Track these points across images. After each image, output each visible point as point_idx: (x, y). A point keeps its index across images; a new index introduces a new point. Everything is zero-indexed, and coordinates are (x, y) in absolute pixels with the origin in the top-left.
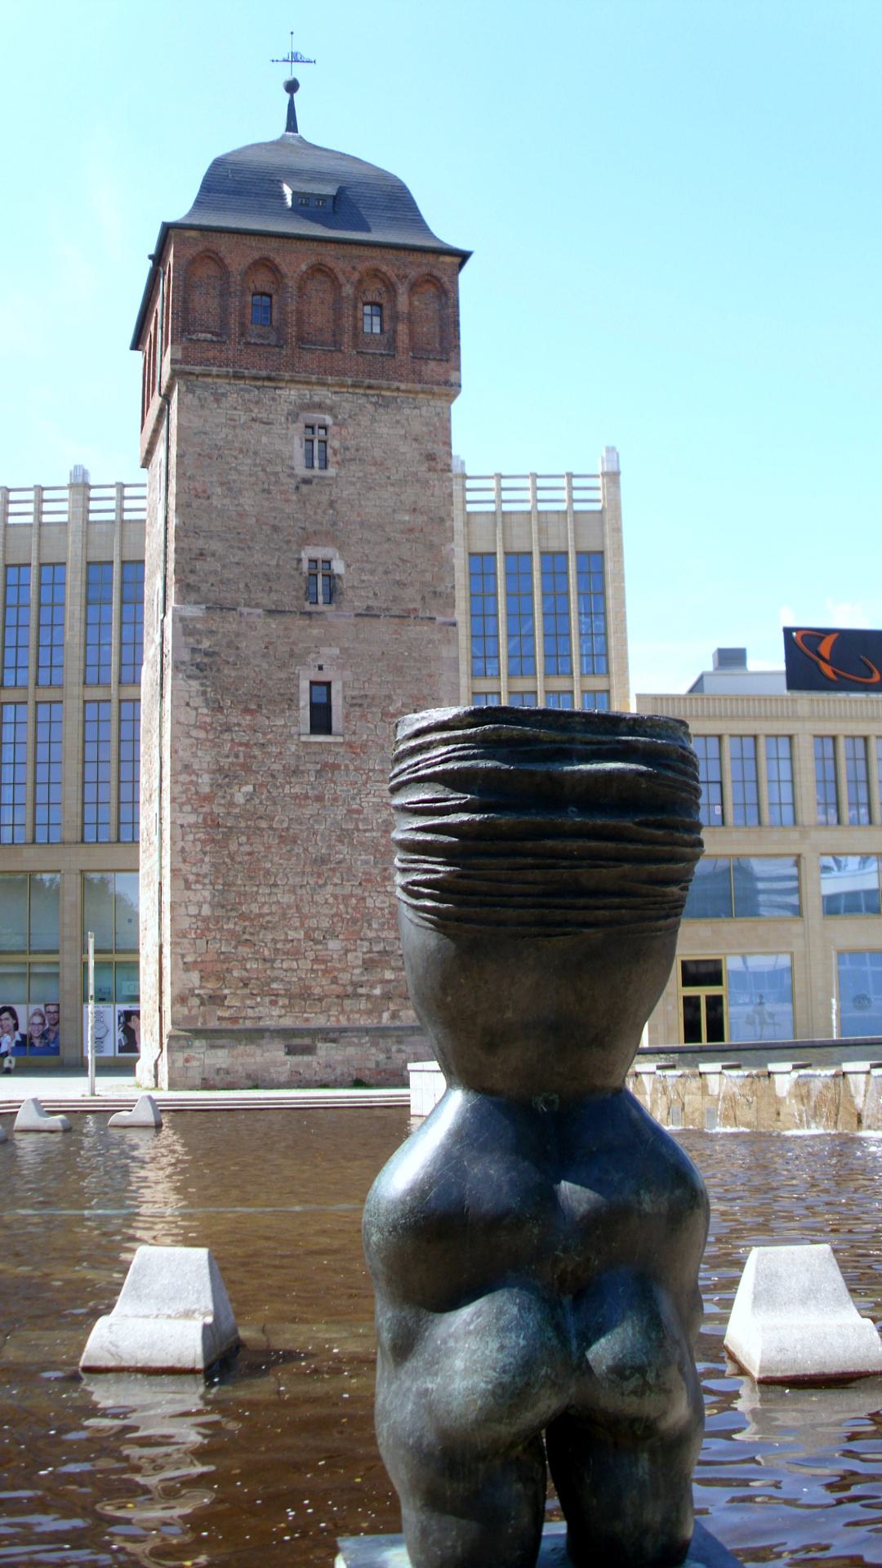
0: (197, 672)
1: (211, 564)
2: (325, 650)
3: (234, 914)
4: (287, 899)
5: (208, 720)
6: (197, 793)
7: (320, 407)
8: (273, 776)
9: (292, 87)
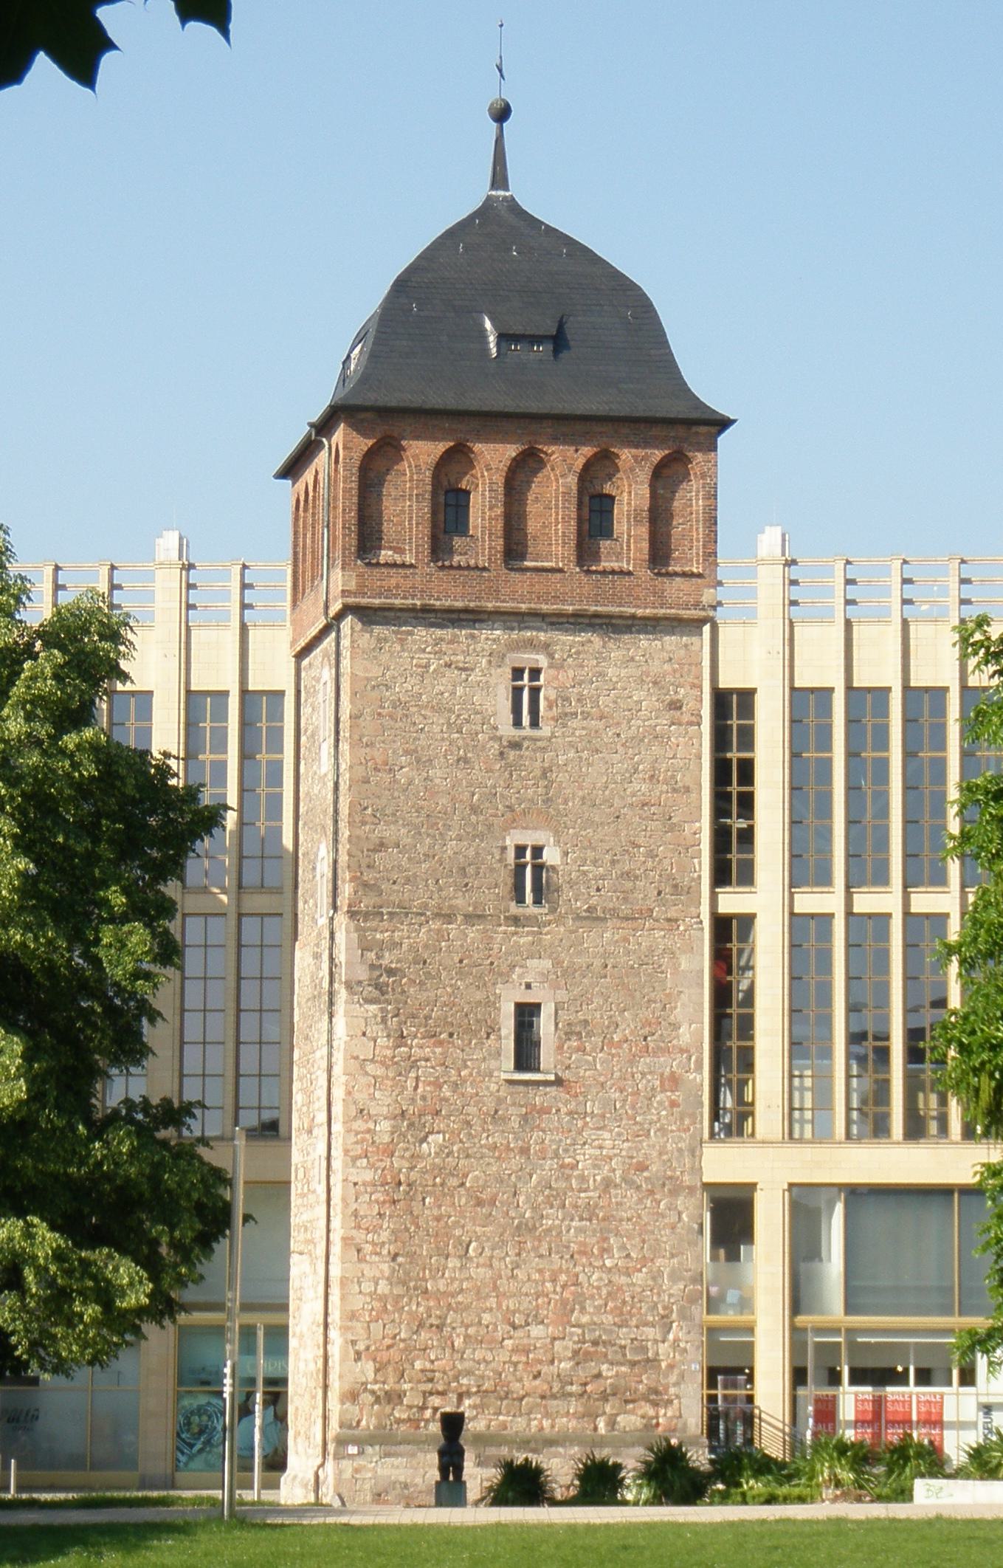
0: (376, 993)
2: (533, 963)
4: (482, 1273)
5: (389, 1053)
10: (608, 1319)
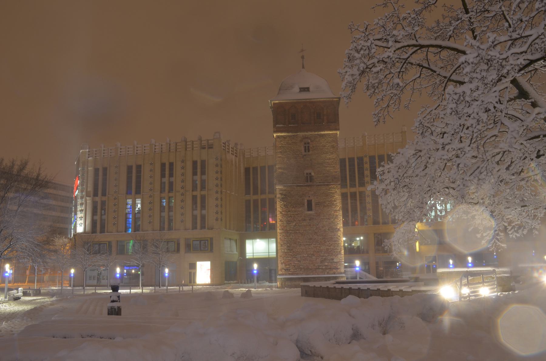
9: (303, 57)
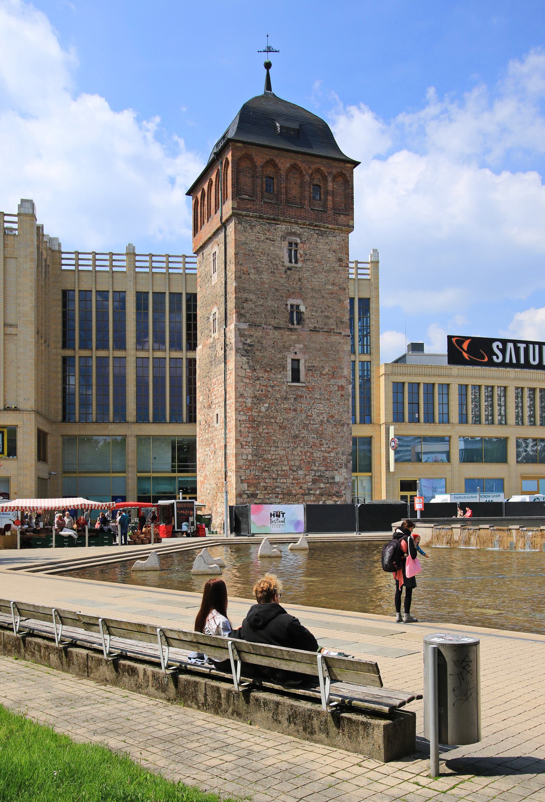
0: (245, 353)
1: (250, 305)
2: (297, 345)
3: (261, 459)
4: (282, 453)
5: (250, 374)
6: (246, 406)
7: (294, 234)
8: (277, 400)
10: (324, 468)
